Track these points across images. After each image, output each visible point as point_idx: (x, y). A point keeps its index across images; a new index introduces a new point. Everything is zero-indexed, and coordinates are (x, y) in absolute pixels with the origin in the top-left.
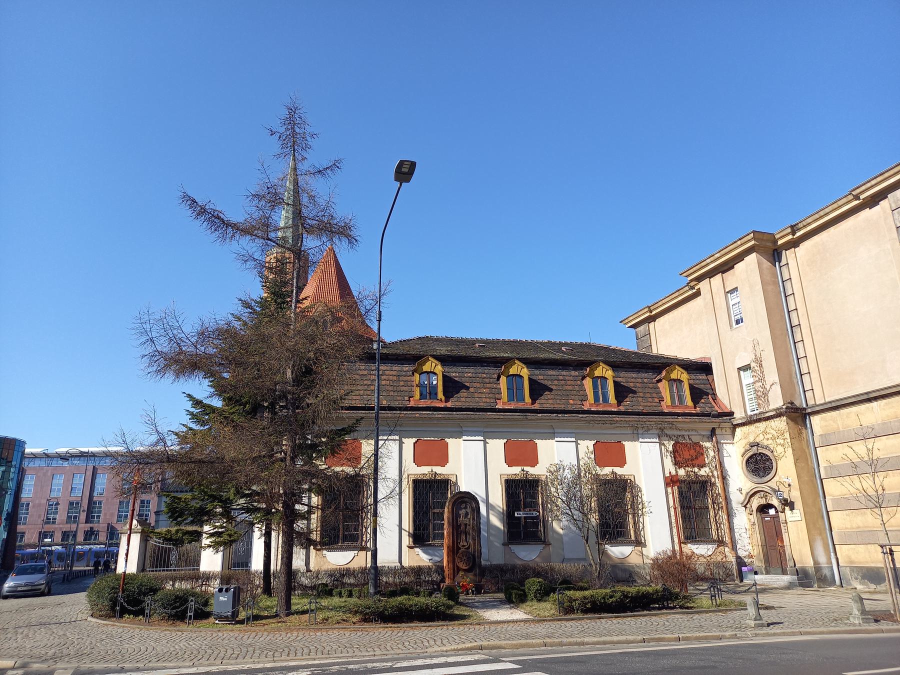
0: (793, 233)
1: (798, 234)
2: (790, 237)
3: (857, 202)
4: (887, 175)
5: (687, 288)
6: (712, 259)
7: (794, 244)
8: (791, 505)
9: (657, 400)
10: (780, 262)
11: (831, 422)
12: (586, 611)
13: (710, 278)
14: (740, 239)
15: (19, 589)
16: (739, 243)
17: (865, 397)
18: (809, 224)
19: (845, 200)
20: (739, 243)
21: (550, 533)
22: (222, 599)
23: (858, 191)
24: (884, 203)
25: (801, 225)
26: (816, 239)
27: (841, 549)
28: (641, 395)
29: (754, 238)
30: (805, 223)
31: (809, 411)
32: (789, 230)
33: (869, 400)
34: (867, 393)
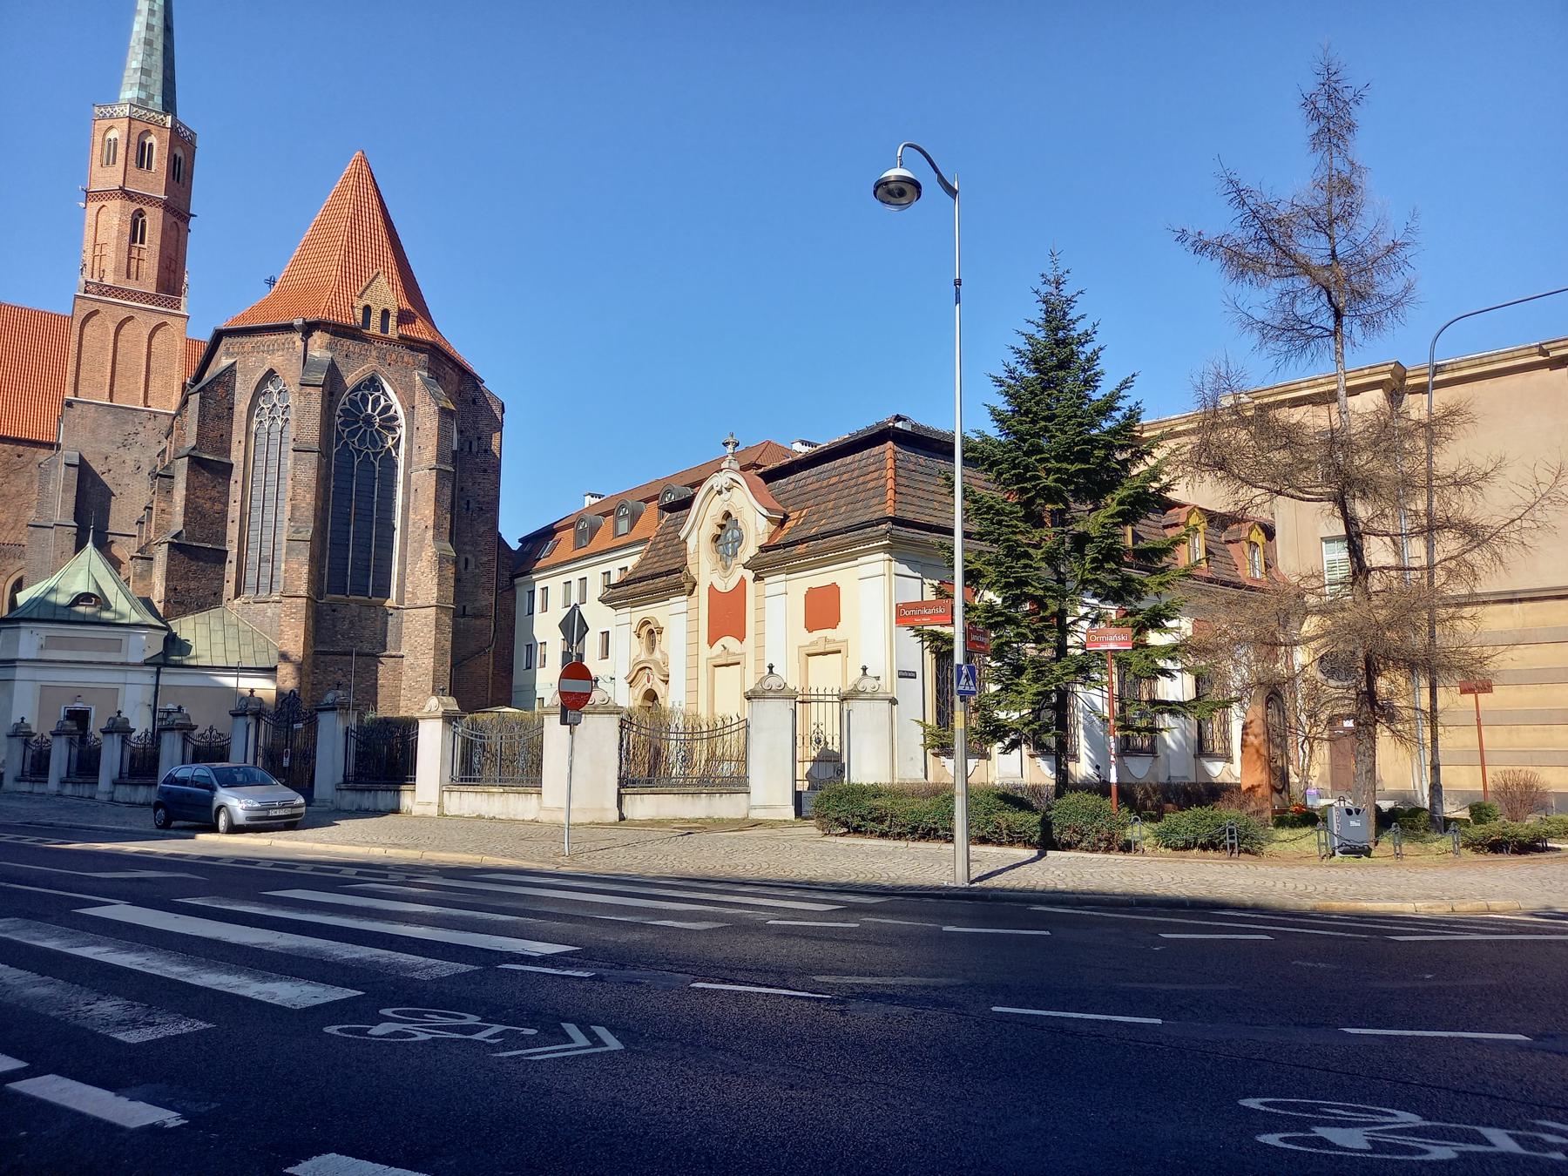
1: (1438, 378)
3: (1541, 358)
6: (1311, 383)
9: (1233, 568)
14: (1370, 368)
15: (272, 813)
16: (1366, 372)
18: (1460, 369)
19: (1526, 352)
20: (1366, 372)
22: (1353, 823)
23: (1553, 345)
28: (1218, 558)
29: (1391, 372)
30: (1455, 366)
33: (1511, 601)
34: (1514, 592)
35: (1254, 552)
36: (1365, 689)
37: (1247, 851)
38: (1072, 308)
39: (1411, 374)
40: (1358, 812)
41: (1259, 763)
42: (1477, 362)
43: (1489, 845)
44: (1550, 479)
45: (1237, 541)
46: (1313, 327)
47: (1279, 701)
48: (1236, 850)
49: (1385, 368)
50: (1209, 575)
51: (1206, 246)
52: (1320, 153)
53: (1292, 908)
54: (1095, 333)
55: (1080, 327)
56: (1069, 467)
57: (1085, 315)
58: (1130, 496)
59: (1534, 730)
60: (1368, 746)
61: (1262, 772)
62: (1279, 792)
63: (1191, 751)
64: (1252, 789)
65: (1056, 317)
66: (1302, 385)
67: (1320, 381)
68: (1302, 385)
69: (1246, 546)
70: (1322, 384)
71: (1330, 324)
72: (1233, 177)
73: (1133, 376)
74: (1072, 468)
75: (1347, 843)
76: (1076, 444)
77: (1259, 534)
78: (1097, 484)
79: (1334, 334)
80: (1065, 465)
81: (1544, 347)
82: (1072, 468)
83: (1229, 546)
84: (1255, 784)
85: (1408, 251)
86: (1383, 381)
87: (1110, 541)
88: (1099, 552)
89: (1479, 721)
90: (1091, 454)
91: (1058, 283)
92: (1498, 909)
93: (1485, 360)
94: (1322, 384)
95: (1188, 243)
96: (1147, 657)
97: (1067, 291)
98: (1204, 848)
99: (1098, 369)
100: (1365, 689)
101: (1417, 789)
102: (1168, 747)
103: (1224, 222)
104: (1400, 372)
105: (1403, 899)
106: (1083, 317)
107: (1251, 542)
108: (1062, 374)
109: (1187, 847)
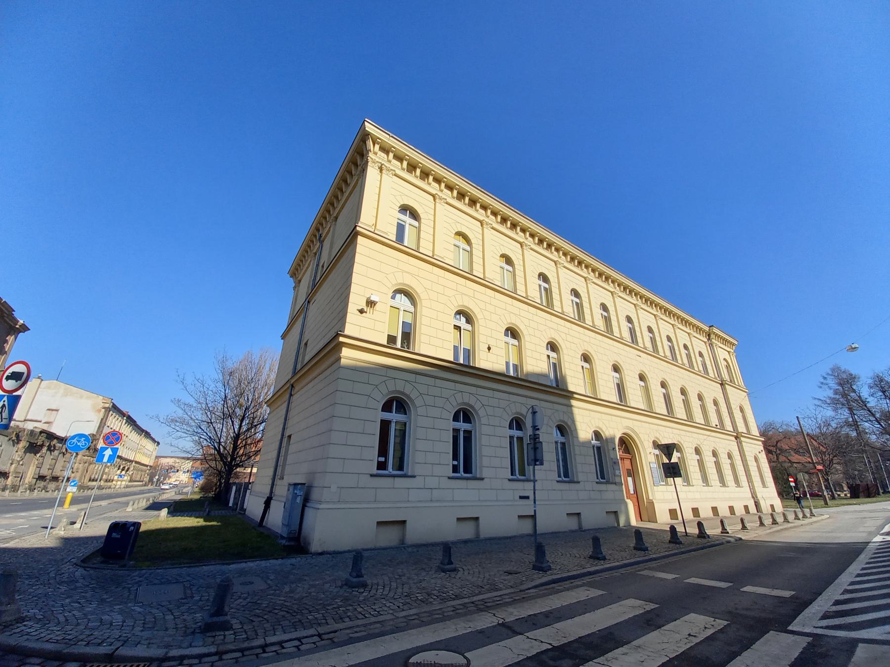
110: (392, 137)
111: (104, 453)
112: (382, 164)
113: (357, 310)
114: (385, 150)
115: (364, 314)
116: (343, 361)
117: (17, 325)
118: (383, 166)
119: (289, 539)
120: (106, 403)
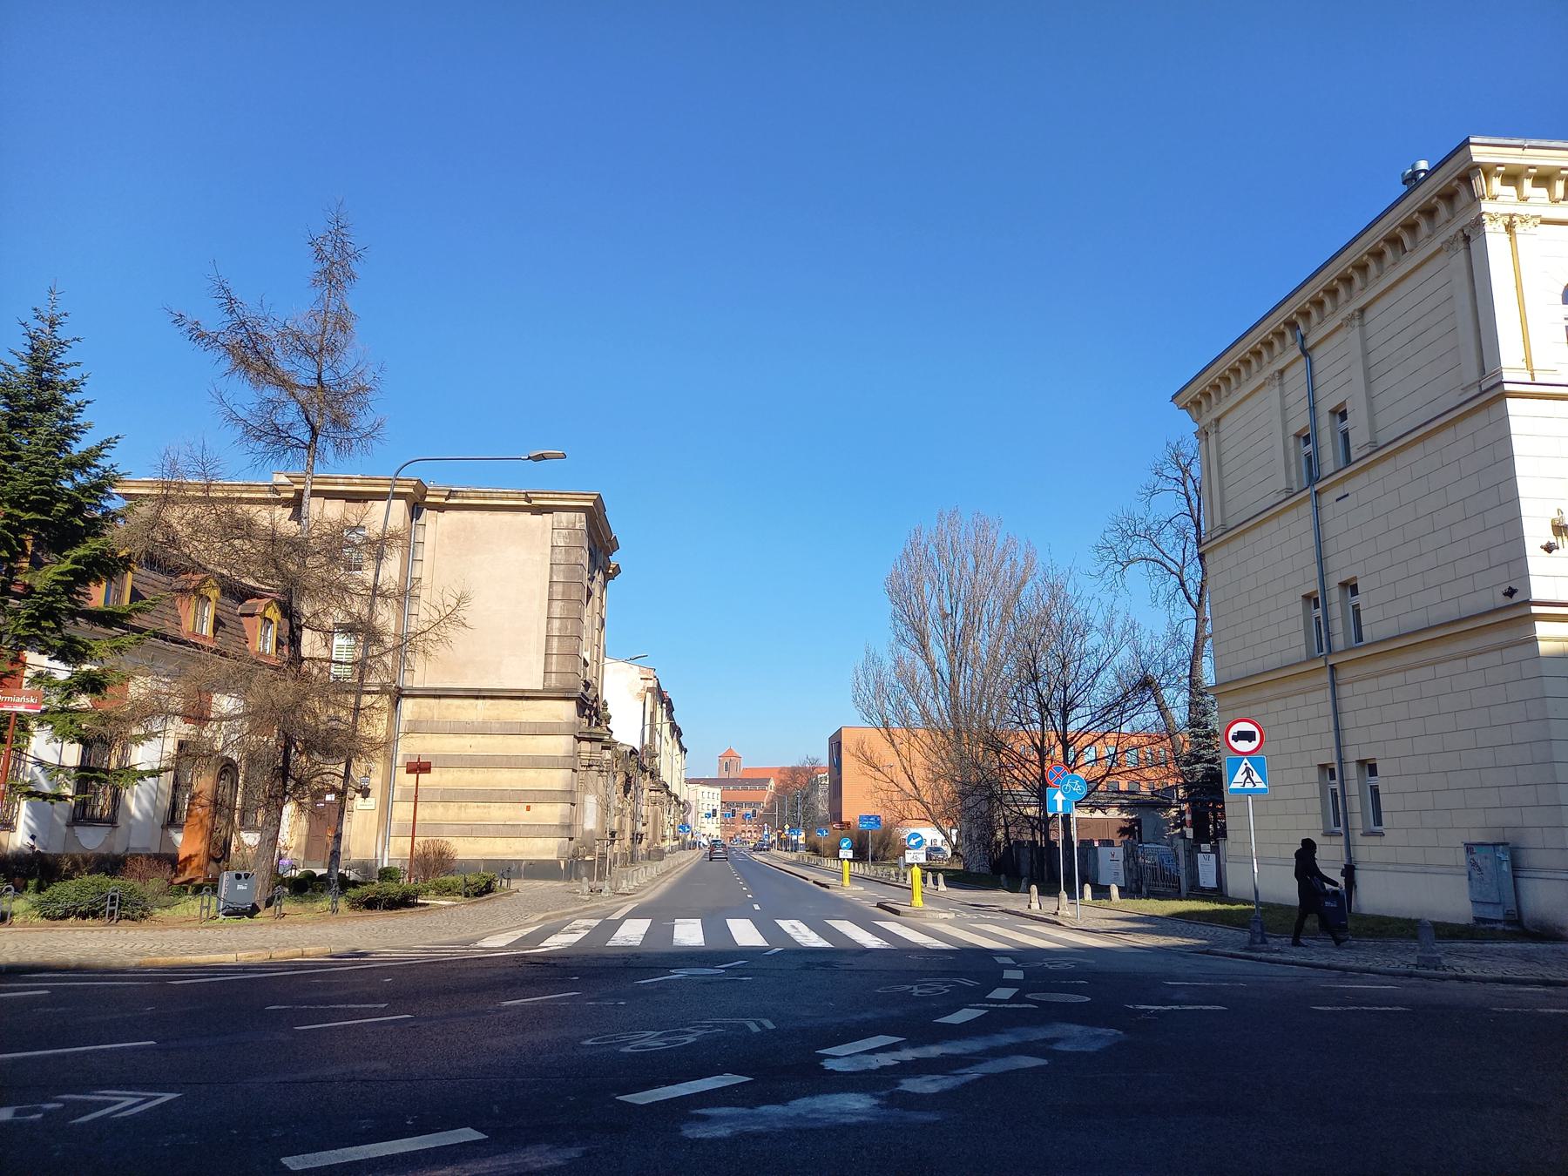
0: (447, 498)
1: (451, 501)
2: (443, 500)
3: (526, 503)
4: (564, 496)
5: (267, 488)
6: (346, 481)
7: (440, 508)
8: (365, 793)
9: (243, 641)
10: (418, 519)
11: (427, 710)
12: (476, 895)
13: (325, 498)
17: (476, 694)
18: (469, 498)
19: (516, 496)
21: (121, 814)
22: (240, 887)
23: (534, 495)
24: (547, 517)
25: (460, 494)
26: (466, 514)
27: (395, 841)
28: (228, 629)
30: (465, 495)
31: (407, 692)
32: (447, 493)
33: (477, 697)
34: (480, 690)
35: (268, 628)
36: (281, 765)
37: (127, 917)
38: (63, 352)
39: (431, 493)
40: (247, 876)
41: (200, 833)
42: (482, 495)
43: (365, 903)
44: (453, 602)
45: (252, 615)
46: (290, 437)
47: (234, 774)
48: (116, 917)
49: (410, 483)
50: (214, 646)
51: (202, 336)
52: (319, 291)
53: (117, 965)
54: (83, 384)
55: (72, 374)
56: (22, 514)
57: (75, 362)
58: (85, 556)
59: (478, 807)
60: (275, 816)
61: (201, 842)
62: (218, 861)
63: (158, 822)
64: (189, 859)
65: (42, 361)
66: (339, 481)
67: (354, 480)
68: (339, 481)
69: (259, 621)
70: (356, 484)
71: (307, 438)
72: (225, 285)
73: (117, 437)
74: (27, 516)
75: (231, 905)
76: (35, 493)
77: (275, 612)
78: (62, 536)
79: (308, 447)
80: (17, 512)
81: (529, 495)
82: (27, 516)
83: (243, 620)
84: (193, 853)
85: (370, 396)
86: (406, 494)
87: (50, 599)
88: (37, 610)
89: (416, 797)
90: (51, 504)
91: (52, 325)
92: (311, 953)
93: (488, 495)
94: (356, 484)
95: (184, 328)
96: (72, 722)
97: (62, 333)
98: (84, 916)
99: (78, 421)
100: (281, 765)
101: (379, 858)
102: (131, 816)
103: (214, 320)
104: (421, 489)
105: (232, 950)
106: (77, 364)
107: (265, 619)
108: (39, 416)
109: (64, 917)
110: (1530, 147)
111: (1055, 798)
112: (1511, 216)
113: (1542, 547)
114: (1512, 177)
115: (1555, 551)
116: (1544, 647)
117: (609, 569)
118: (1515, 219)
119: (1509, 923)
120: (647, 679)
